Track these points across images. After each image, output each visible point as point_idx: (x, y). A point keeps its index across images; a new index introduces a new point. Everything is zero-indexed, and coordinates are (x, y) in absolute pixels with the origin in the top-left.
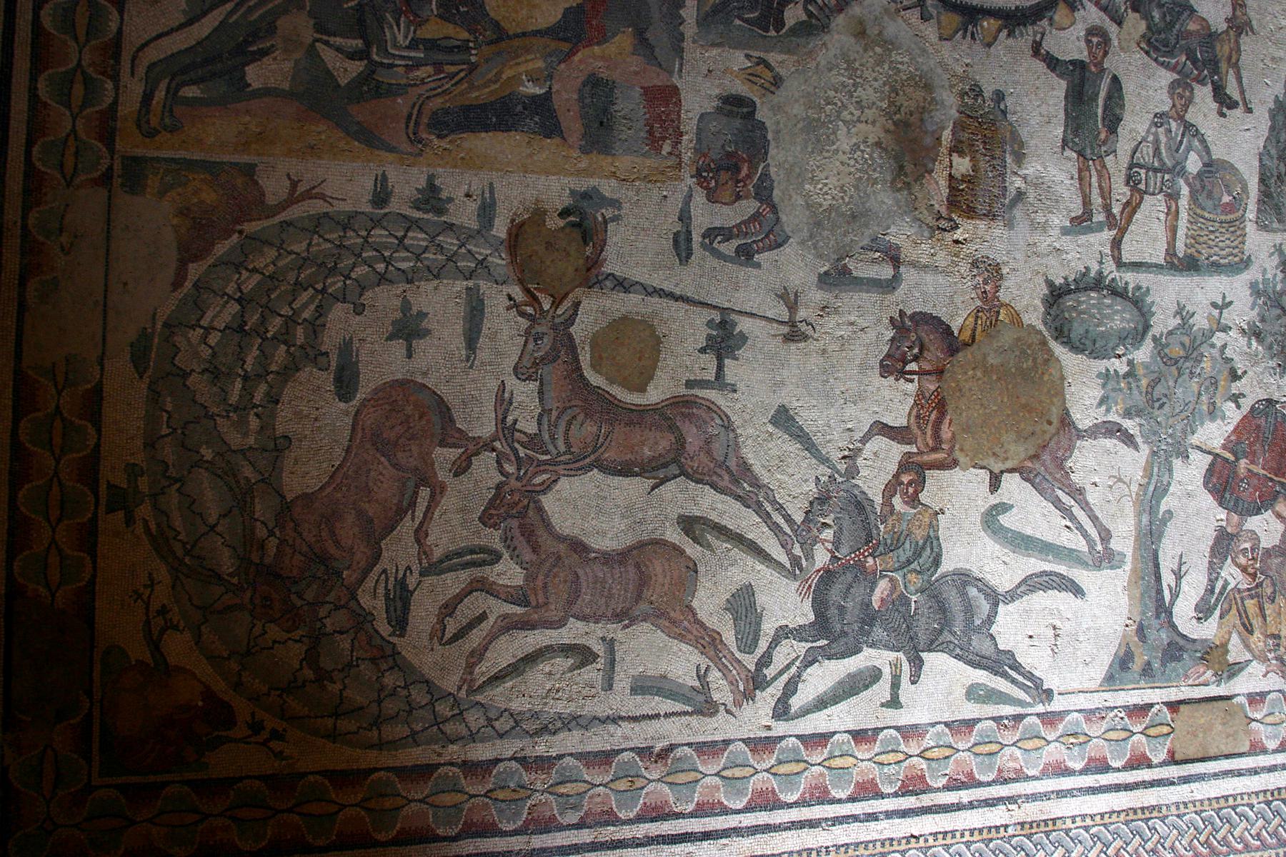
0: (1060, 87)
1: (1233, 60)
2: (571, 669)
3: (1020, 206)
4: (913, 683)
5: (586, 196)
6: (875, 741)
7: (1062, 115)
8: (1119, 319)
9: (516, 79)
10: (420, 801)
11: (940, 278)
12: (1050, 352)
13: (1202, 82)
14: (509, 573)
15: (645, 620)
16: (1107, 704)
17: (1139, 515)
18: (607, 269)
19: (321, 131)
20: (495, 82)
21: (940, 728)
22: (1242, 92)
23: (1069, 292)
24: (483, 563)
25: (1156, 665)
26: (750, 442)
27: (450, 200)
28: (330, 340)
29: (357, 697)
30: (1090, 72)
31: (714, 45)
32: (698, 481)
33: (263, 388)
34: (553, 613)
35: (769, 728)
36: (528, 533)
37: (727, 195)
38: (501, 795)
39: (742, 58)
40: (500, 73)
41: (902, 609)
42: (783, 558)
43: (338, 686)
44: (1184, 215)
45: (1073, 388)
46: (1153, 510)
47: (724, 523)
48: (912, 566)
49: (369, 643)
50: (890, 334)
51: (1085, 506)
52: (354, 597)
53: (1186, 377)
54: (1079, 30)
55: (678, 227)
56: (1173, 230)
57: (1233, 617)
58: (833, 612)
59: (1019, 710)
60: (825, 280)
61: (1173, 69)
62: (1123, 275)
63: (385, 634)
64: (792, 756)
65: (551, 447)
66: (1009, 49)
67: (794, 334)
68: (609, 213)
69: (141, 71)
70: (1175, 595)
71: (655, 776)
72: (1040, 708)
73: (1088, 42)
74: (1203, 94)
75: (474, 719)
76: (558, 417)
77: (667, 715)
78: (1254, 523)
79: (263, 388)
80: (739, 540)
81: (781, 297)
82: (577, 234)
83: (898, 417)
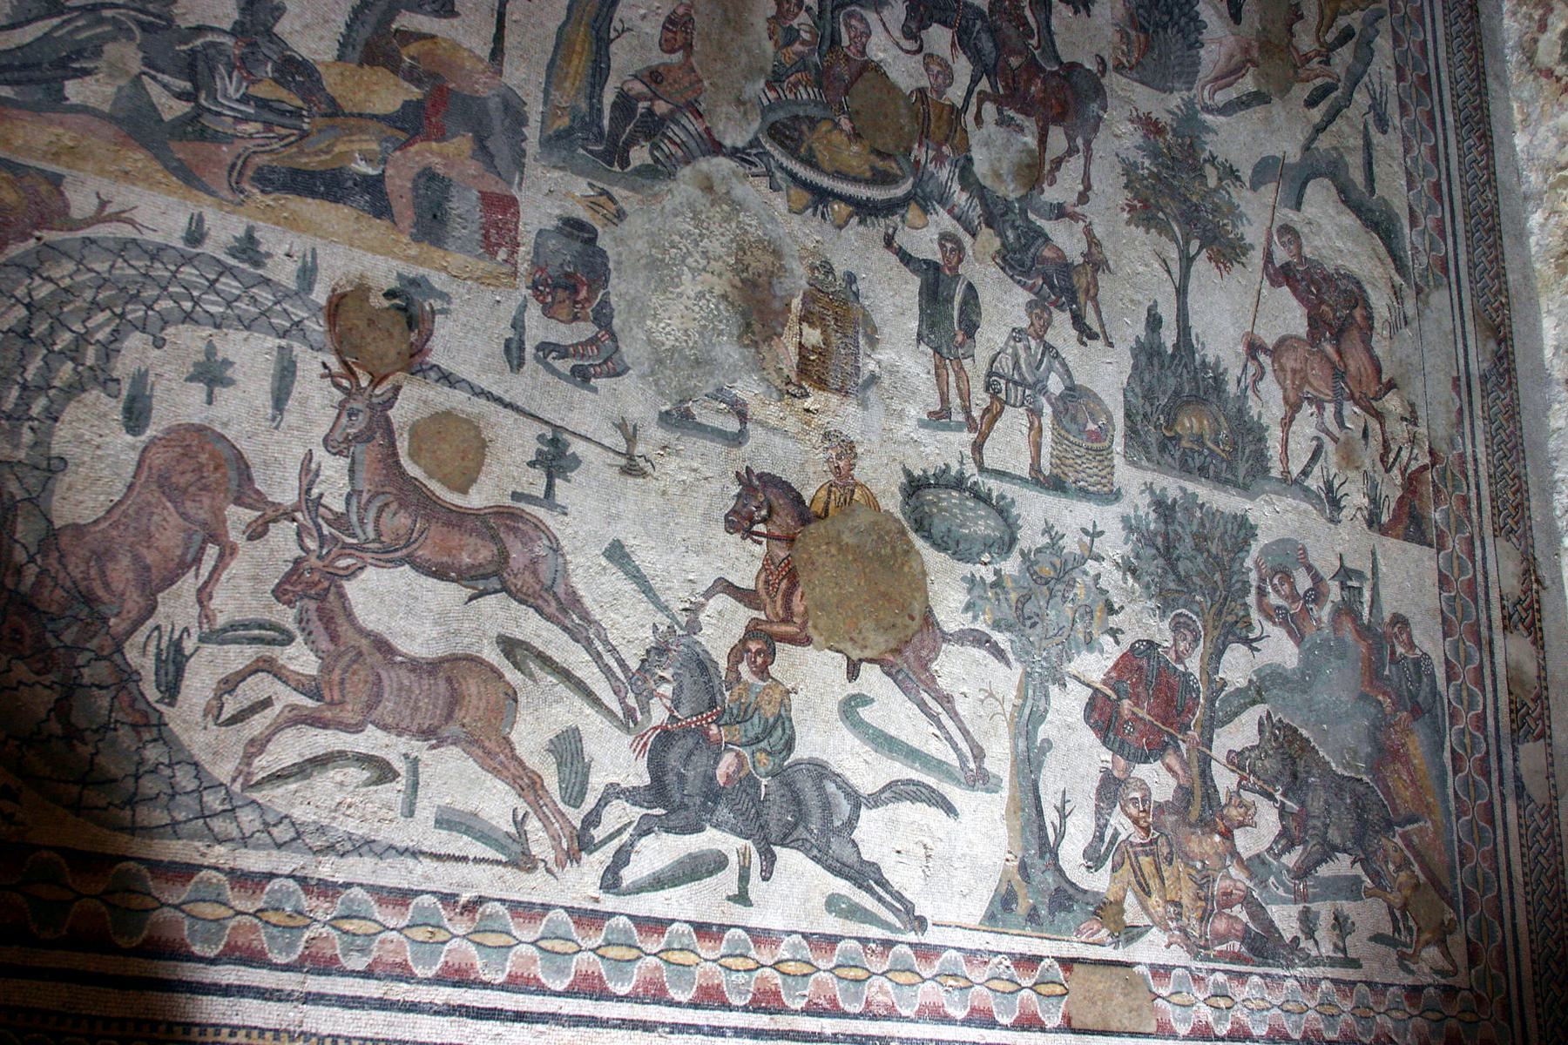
0: (914, 284)
1: (1092, 293)
2: (367, 784)
3: (874, 388)
4: (765, 879)
5: (414, 282)
6: (721, 940)
7: (916, 310)
8: (984, 525)
9: (348, 155)
12: (909, 542)
13: (1061, 308)
15: (454, 743)
16: (990, 948)
17: (1014, 738)
18: (432, 359)
19: (137, 159)
20: (327, 153)
21: (797, 938)
22: (1102, 326)
23: (929, 486)
26: (580, 571)
27: (269, 255)
28: (124, 367)
29: (110, 764)
31: (554, 167)
32: (521, 602)
34: (349, 714)
35: (596, 900)
36: (327, 620)
37: (564, 312)
39: (585, 185)
40: (332, 145)
41: (751, 791)
42: (615, 707)
44: (1048, 435)
45: (936, 587)
46: (1030, 736)
47: (549, 653)
48: (763, 744)
49: (132, 706)
51: (954, 716)
52: (119, 649)
53: (1058, 599)
55: (510, 334)
56: (1037, 447)
58: (671, 778)
61: (1030, 289)
63: (151, 699)
64: (622, 939)
65: (359, 531)
66: (861, 236)
67: (631, 468)
68: (437, 305)
70: (1060, 835)
71: (461, 931)
72: (912, 937)
73: (942, 246)
74: (1062, 319)
75: (248, 819)
76: (369, 501)
78: (1142, 771)
80: (565, 675)
82: (402, 318)
83: (746, 578)
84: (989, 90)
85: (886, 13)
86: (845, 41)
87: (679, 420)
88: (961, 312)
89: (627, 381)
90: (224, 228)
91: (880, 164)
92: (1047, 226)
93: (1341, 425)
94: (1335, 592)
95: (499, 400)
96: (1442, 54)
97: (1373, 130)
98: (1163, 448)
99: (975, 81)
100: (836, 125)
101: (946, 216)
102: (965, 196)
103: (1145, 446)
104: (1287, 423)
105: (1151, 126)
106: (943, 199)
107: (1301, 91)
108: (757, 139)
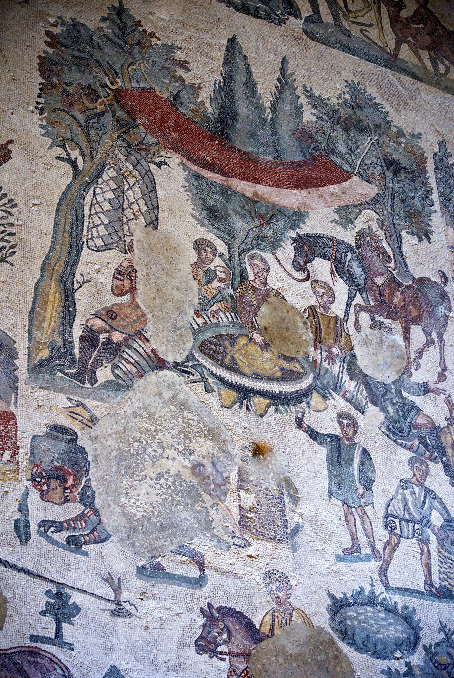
7: (326, 472)
13: (434, 460)
23: (349, 605)
30: (344, 444)
50: (201, 621)
54: (332, 414)
56: (428, 566)
61: (410, 449)
62: (392, 596)
73: (340, 423)
81: (107, 580)
84: (363, 304)
85: (279, 253)
88: (360, 471)
91: (287, 366)
99: (351, 298)
100: (251, 339)
101: (341, 400)
102: (353, 383)
106: (337, 388)
108: (192, 354)
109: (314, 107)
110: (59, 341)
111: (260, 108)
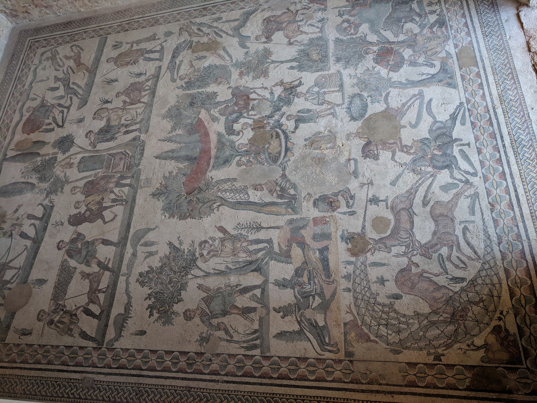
0: (301, 125)
2: (470, 232)
5: (342, 238)
10: (516, 271)
11: (352, 148)
13: (296, 90)
14: (444, 251)
17: (408, 88)
19: (333, 306)
22: (297, 80)
23: (352, 115)
24: (442, 258)
25: (449, 76)
27: (347, 272)
28: (387, 301)
29: (486, 291)
33: (401, 319)
34: (454, 238)
35: (480, 177)
38: (511, 249)
42: (431, 179)
43: (484, 296)
46: (406, 84)
50: (368, 159)
51: (407, 102)
54: (287, 122)
55: (347, 215)
56: (333, 91)
57: (433, 58)
59: (467, 110)
60: (356, 177)
67: (371, 183)
68: (346, 232)
69: (323, 353)
70: (429, 74)
72: (465, 105)
73: (290, 120)
74: (299, 89)
75: (488, 258)
77: (480, 205)
78: (406, 57)
79: (401, 319)
80: (427, 191)
83: (390, 154)
86: (246, 149)
87: (355, 174)
89: (350, 187)
90: (344, 284)
92: (276, 96)
93: (303, 20)
94: (346, 17)
95: (365, 215)
96: (195, 5)
97: (222, 21)
98: (323, 62)
99: (245, 117)
100: (268, 148)
103: (325, 66)
104: (307, 33)
105: (241, 74)
107: (219, 39)
109: (176, 130)
110: (284, 206)
111: (181, 148)
